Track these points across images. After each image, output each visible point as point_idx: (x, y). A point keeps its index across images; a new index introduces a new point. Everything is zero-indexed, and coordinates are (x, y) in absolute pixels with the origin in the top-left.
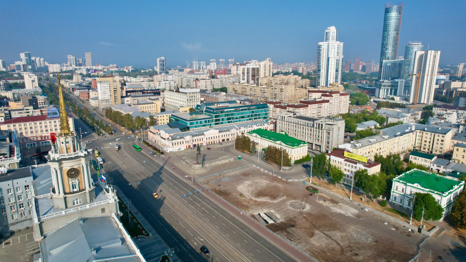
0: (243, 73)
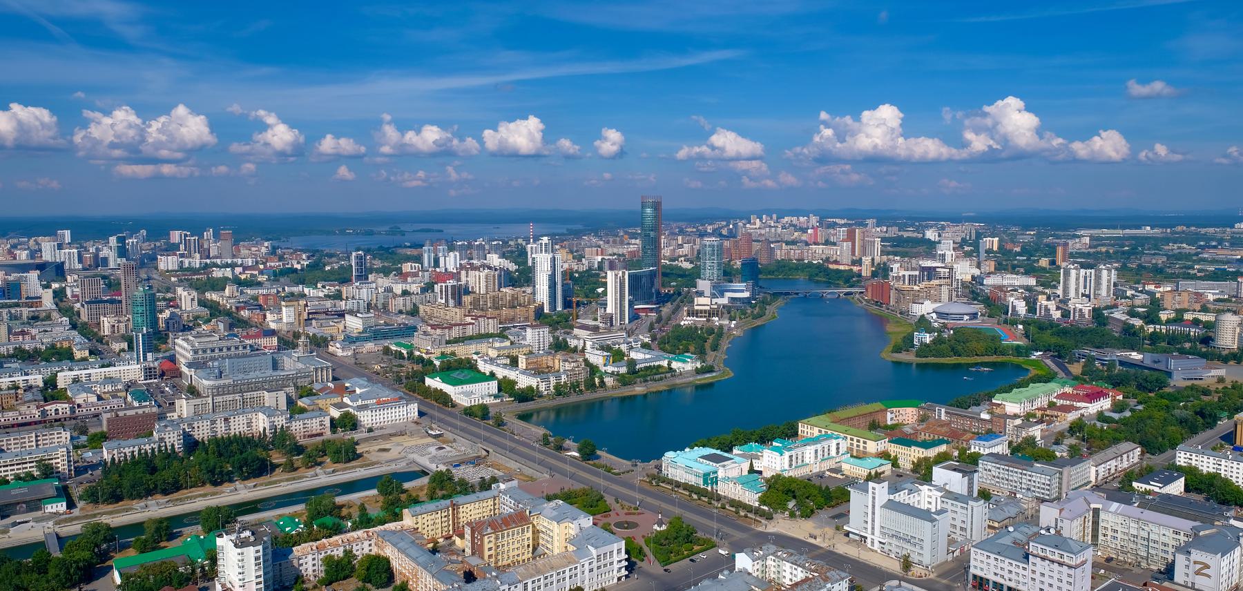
0: (441, 291)
